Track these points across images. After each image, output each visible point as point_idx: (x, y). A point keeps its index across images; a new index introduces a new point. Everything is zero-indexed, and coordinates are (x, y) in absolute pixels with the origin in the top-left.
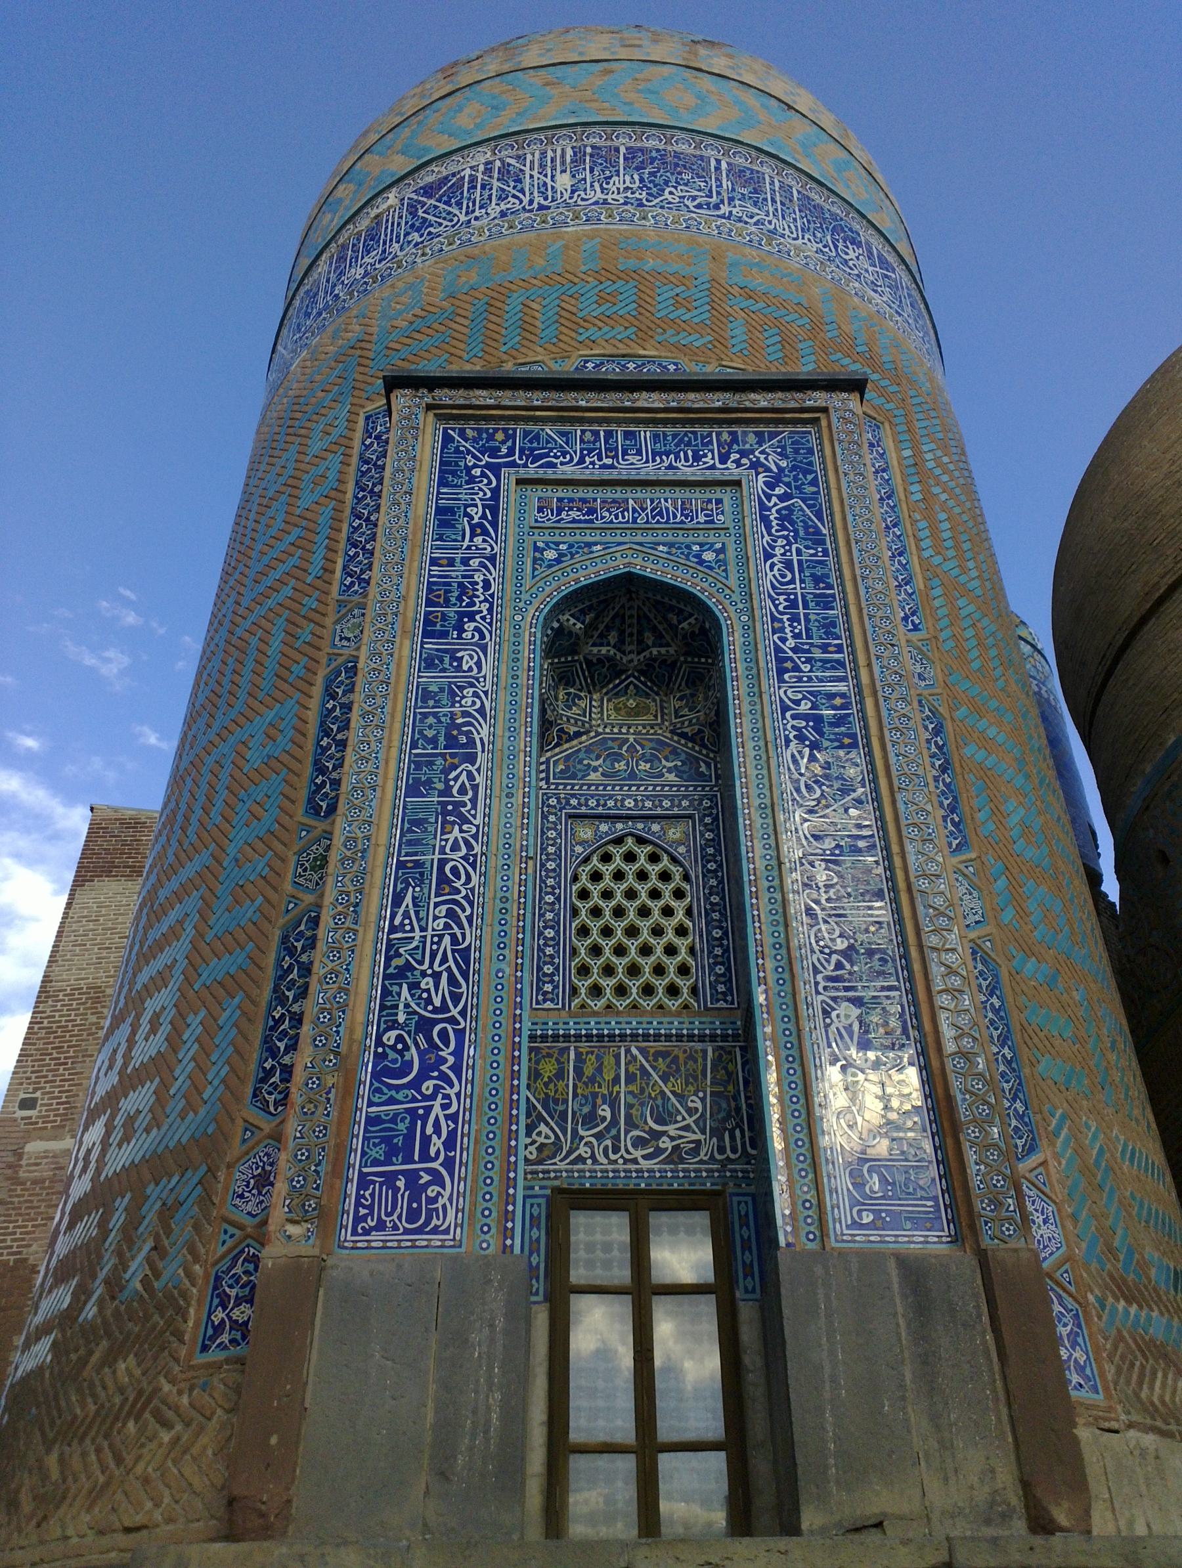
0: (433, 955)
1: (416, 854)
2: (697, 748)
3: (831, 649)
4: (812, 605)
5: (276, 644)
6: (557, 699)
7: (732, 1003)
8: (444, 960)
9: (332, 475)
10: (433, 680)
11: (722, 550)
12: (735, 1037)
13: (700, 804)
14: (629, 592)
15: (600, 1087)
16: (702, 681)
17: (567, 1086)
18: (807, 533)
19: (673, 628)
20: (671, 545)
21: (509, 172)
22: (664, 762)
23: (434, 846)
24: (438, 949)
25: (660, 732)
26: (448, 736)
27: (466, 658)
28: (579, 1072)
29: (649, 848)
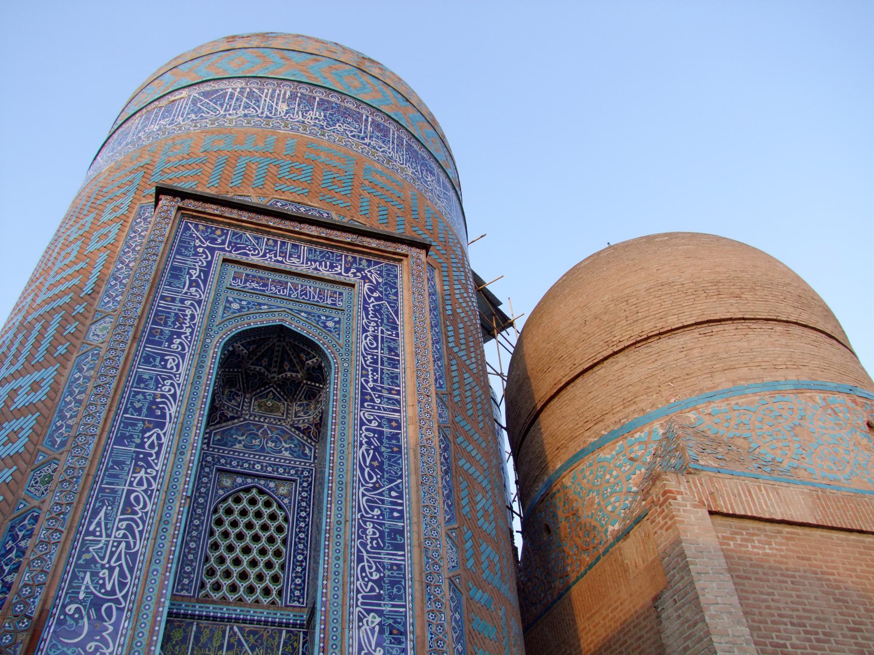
0: (112, 554)
1: (112, 484)
2: (305, 438)
3: (394, 392)
4: (386, 364)
5: (51, 331)
6: (223, 393)
7: (303, 603)
8: (119, 559)
9: (112, 235)
11: (338, 322)
12: (301, 626)
13: (302, 473)
14: (279, 336)
15: (209, 651)
16: (315, 396)
17: (188, 648)
18: (388, 322)
19: (302, 363)
20: (309, 314)
21: (253, 95)
22: (283, 444)
23: (126, 481)
24: (116, 551)
25: (284, 424)
26: (150, 409)
27: (171, 360)
28: (197, 639)
29: (266, 497)
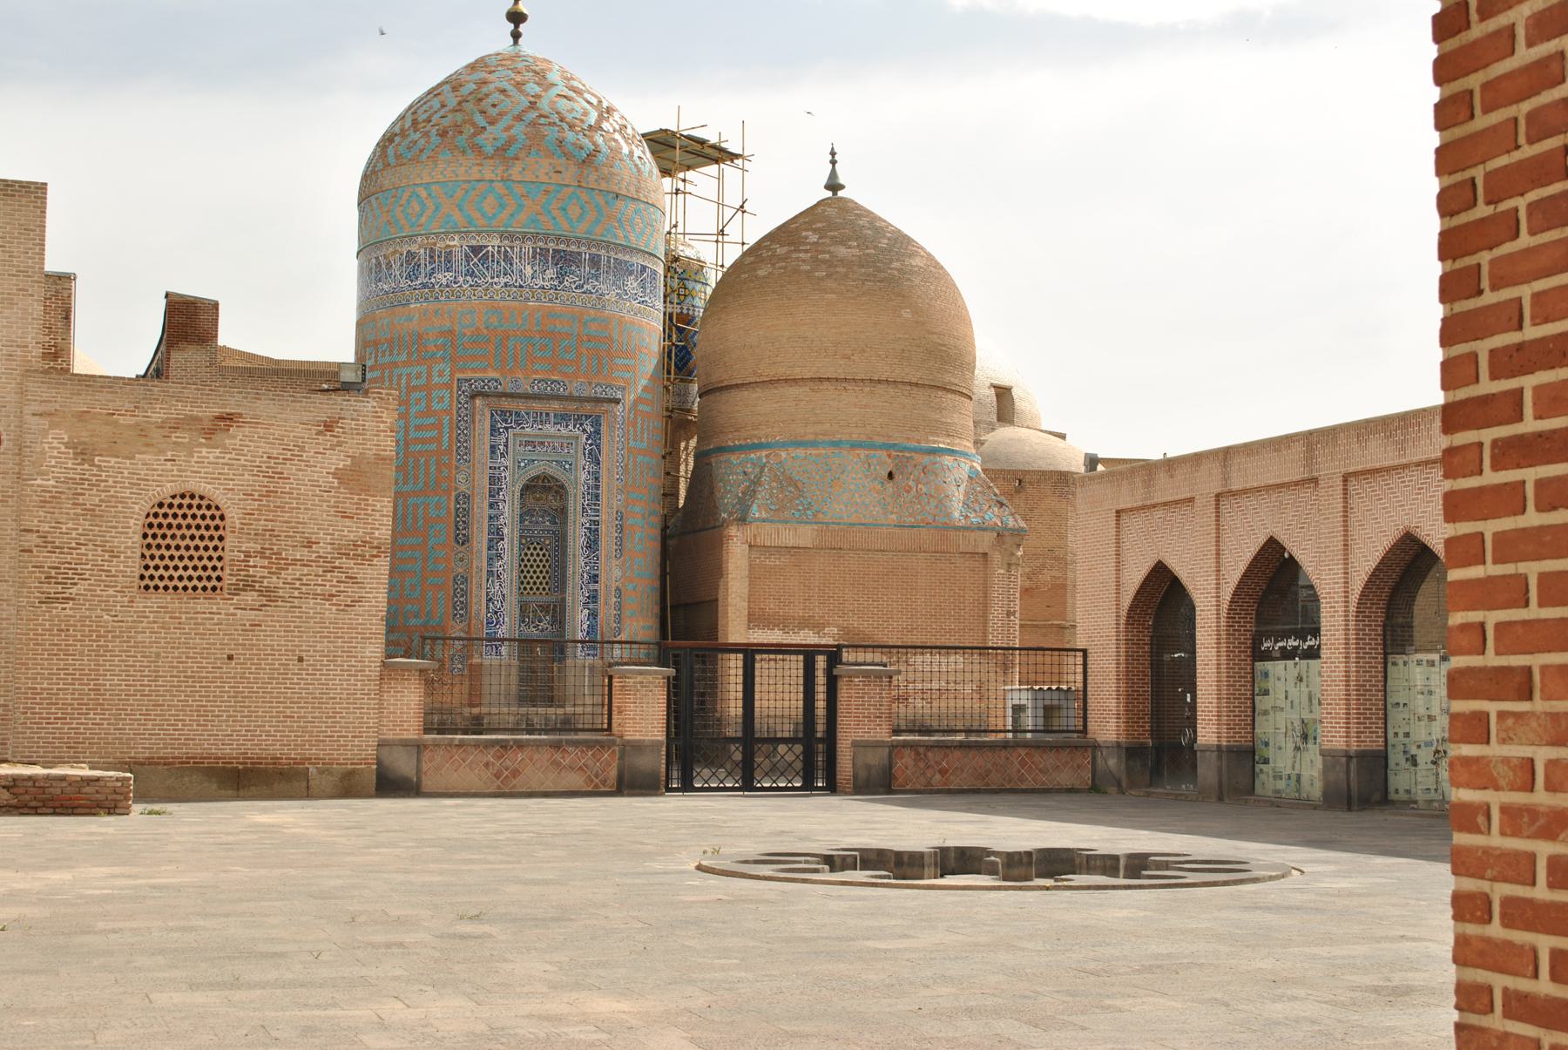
10: (493, 512)
